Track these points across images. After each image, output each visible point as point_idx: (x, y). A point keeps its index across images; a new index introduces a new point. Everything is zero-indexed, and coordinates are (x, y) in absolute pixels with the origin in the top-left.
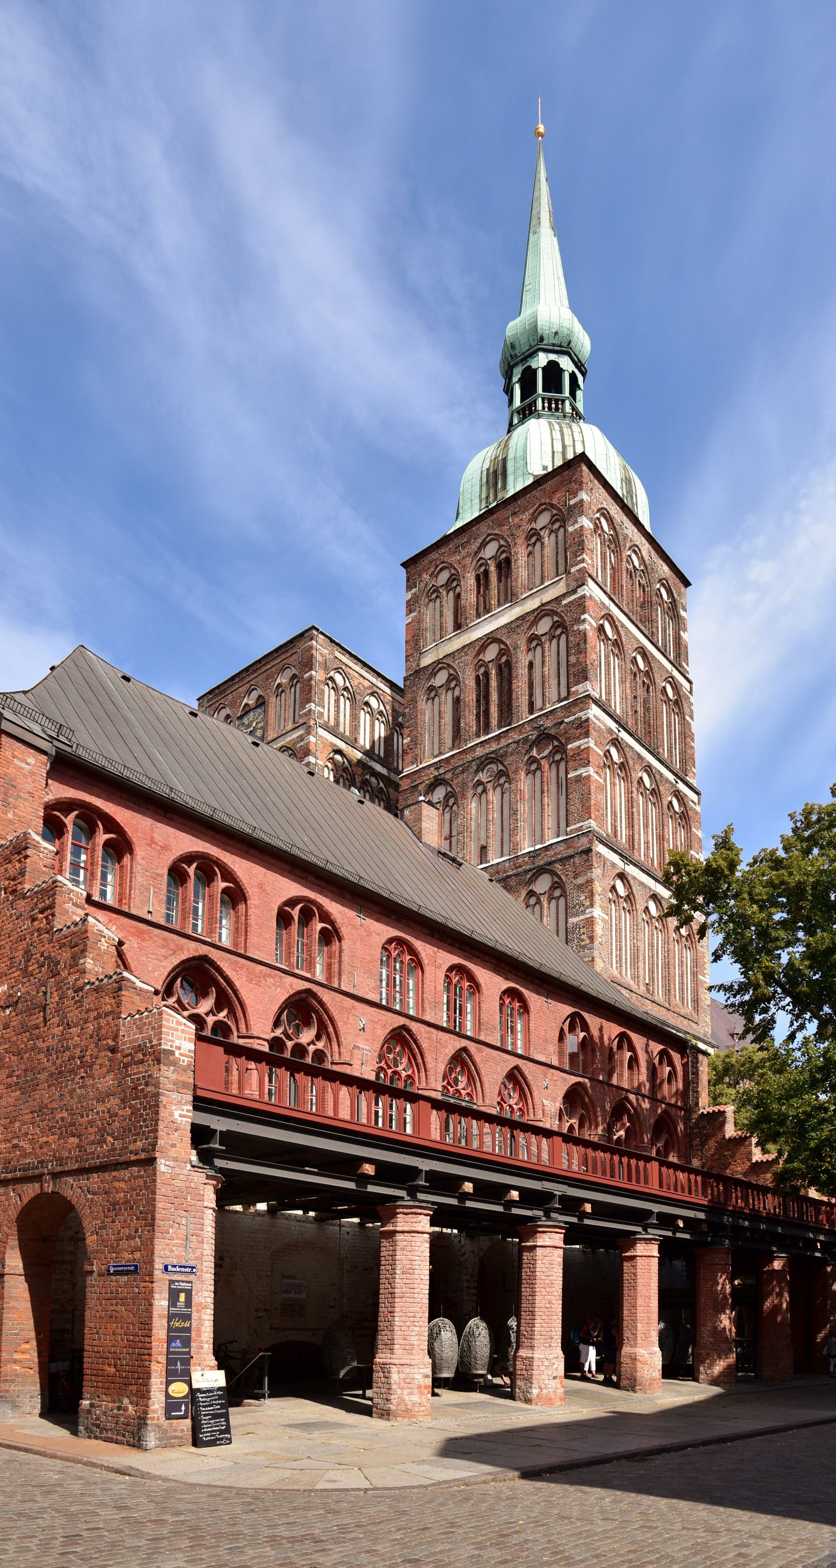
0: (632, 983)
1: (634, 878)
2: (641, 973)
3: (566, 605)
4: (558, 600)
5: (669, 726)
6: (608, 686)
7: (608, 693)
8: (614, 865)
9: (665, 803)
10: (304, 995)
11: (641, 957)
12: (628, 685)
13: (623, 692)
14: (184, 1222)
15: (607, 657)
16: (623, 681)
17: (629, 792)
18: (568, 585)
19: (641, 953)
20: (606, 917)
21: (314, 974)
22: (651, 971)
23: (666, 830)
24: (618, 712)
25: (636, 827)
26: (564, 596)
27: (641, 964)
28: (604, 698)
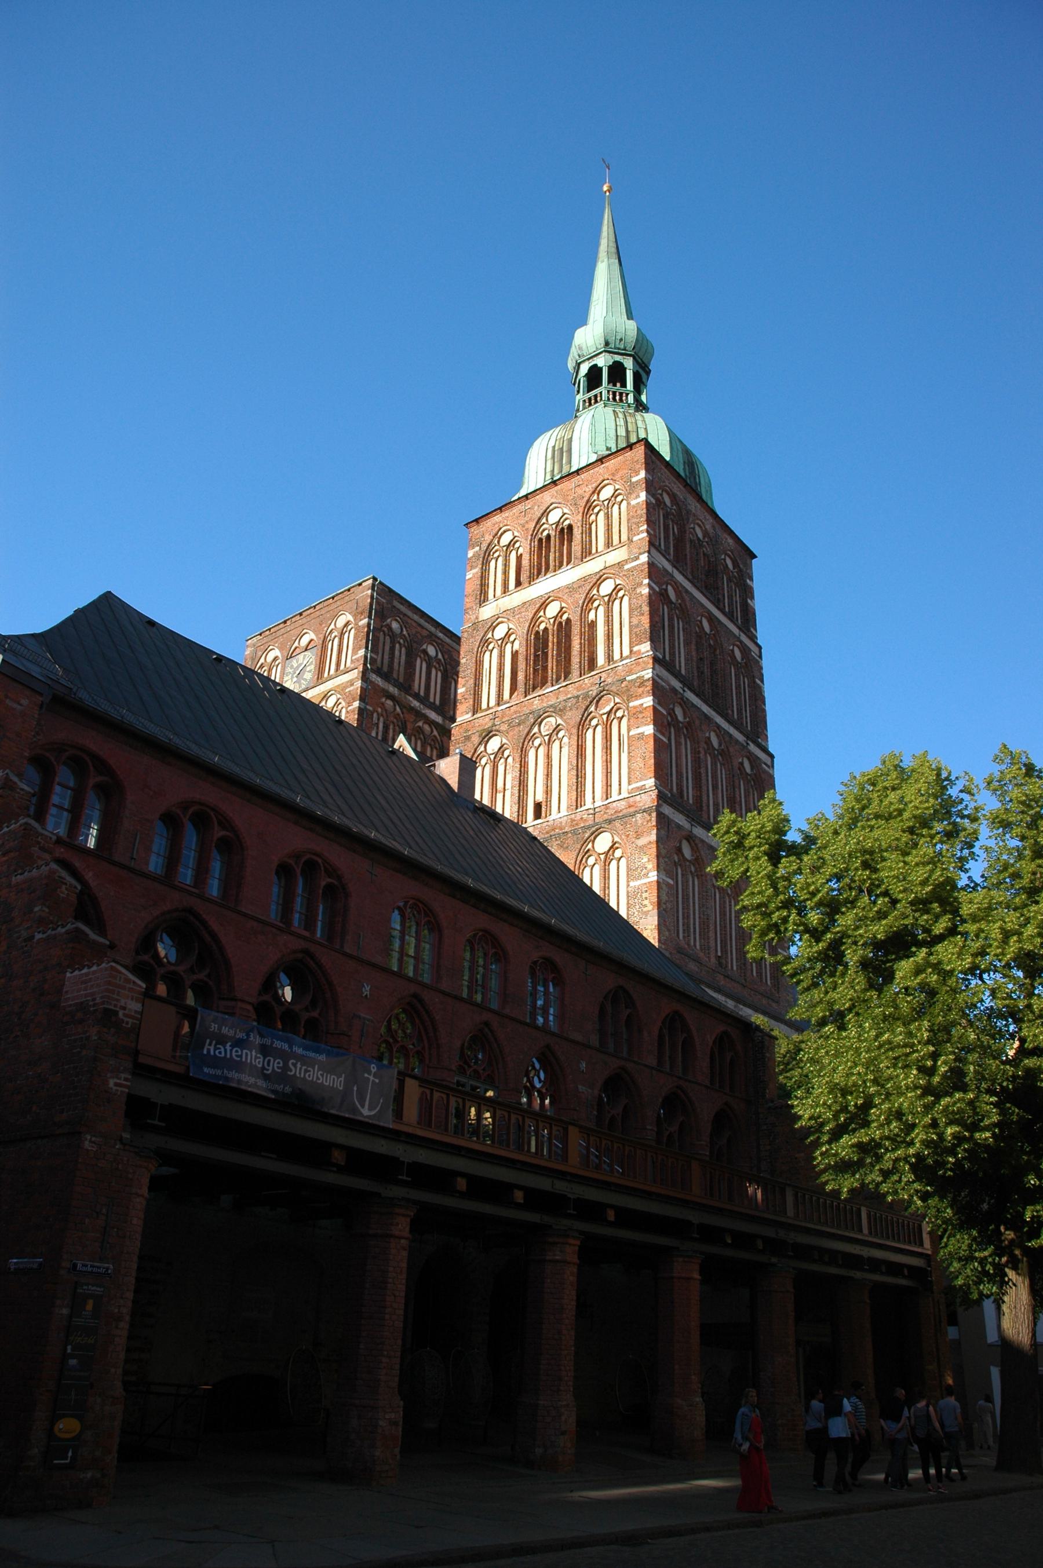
0: (701, 954)
1: (703, 841)
2: (712, 943)
3: (628, 570)
4: (620, 565)
5: (738, 687)
6: (672, 647)
7: (672, 654)
8: (679, 827)
9: (736, 764)
10: (300, 956)
11: (712, 927)
12: (693, 647)
13: (687, 654)
14: (104, 1211)
15: (671, 619)
16: (687, 643)
17: (695, 752)
18: (630, 552)
19: (712, 922)
20: (671, 882)
21: (314, 932)
22: (724, 943)
23: (737, 792)
24: (683, 672)
25: (704, 788)
26: (626, 561)
27: (711, 934)
28: (667, 658)
